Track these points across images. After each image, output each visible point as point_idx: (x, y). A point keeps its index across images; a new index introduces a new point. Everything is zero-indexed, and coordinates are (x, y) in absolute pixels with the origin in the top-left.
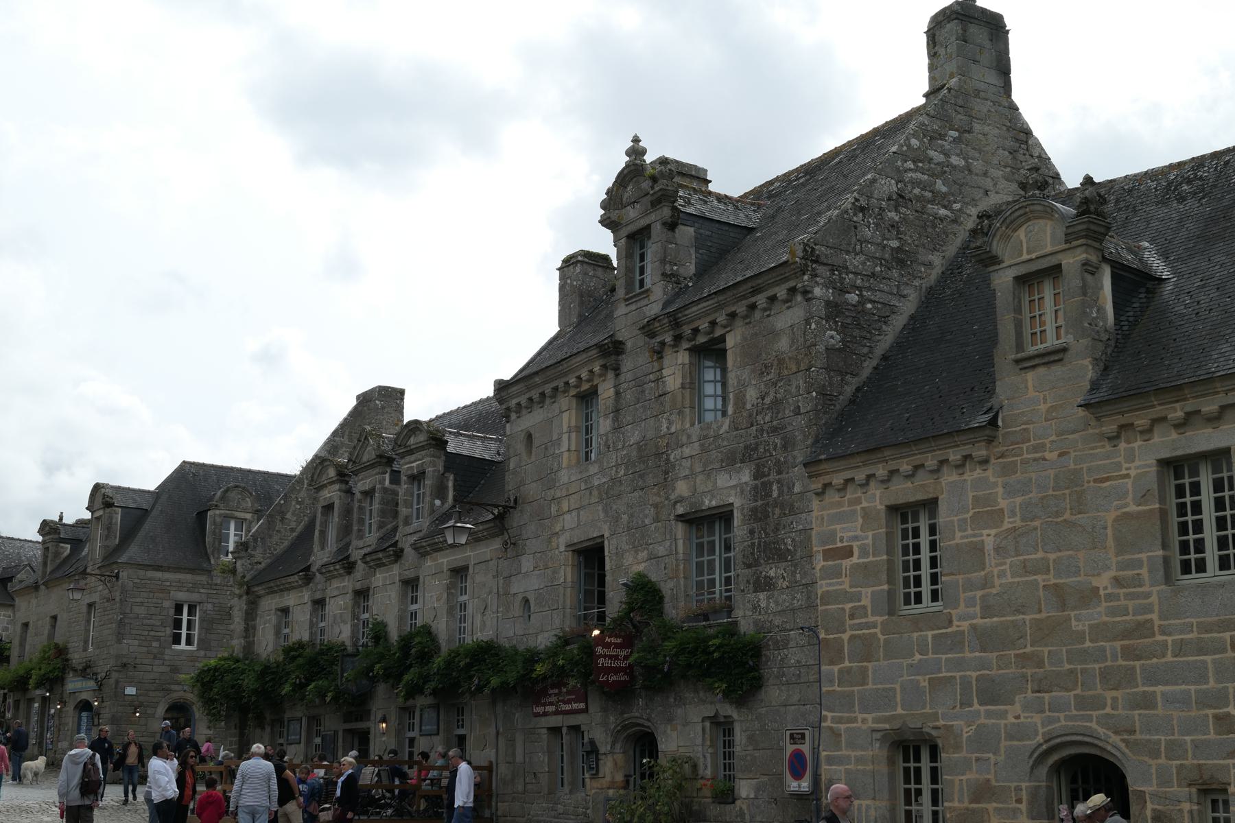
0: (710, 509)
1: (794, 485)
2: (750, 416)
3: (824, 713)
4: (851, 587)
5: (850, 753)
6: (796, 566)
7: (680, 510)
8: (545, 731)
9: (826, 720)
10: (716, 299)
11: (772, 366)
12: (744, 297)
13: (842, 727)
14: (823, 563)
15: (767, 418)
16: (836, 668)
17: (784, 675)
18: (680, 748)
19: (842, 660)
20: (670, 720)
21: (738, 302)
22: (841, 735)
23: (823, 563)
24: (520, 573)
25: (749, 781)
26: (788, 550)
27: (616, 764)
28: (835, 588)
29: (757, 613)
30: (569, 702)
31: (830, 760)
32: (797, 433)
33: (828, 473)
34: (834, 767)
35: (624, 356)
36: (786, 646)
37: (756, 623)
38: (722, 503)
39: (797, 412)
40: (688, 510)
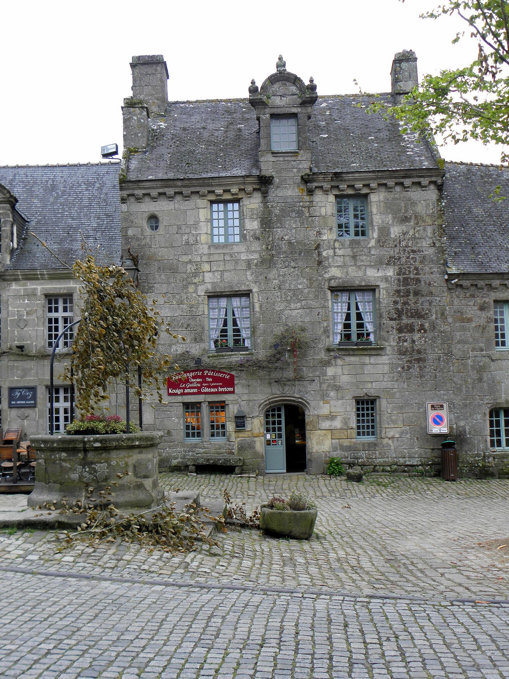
7: (333, 283)
11: (410, 218)
12: (396, 178)
30: (216, 387)
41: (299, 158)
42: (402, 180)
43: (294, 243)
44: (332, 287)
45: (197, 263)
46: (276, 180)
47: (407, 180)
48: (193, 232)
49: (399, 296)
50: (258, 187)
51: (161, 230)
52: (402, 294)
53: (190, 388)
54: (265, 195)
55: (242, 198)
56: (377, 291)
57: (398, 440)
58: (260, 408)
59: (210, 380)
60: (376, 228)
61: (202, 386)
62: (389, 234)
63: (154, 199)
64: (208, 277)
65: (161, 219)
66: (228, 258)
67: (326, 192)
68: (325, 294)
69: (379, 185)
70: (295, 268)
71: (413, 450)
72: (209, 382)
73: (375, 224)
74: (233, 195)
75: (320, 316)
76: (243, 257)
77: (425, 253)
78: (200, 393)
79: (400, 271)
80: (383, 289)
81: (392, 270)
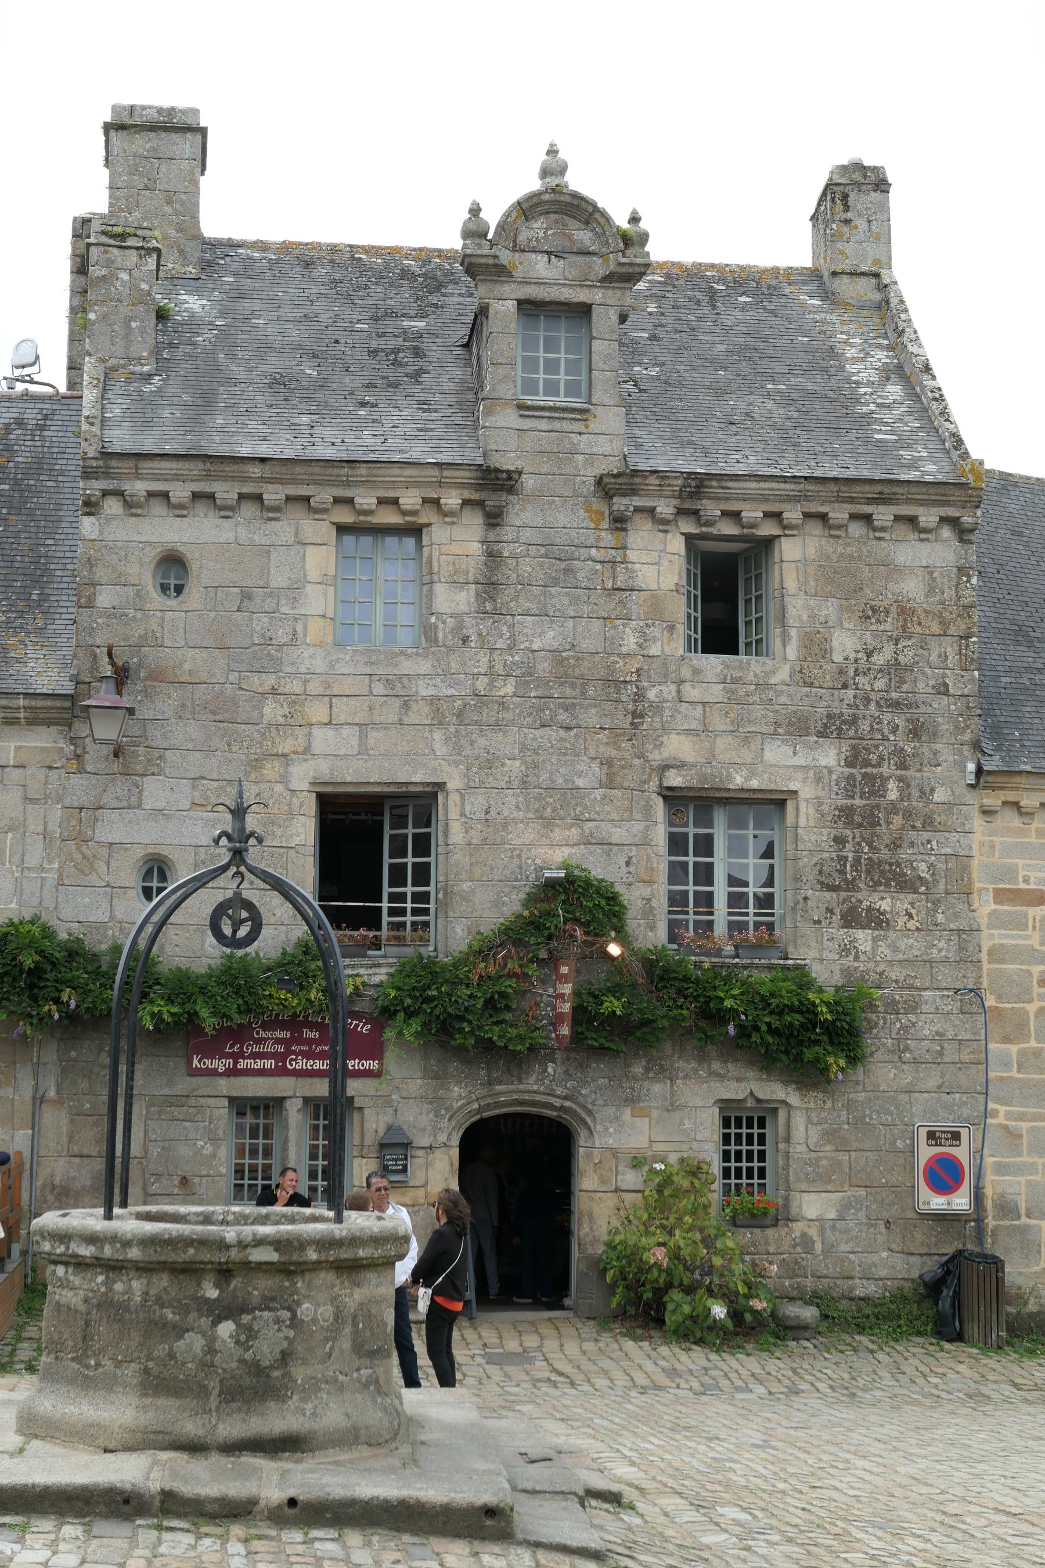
0: (742, 790)
1: (933, 790)
2: (841, 672)
3: (991, 1105)
4: (1041, 944)
5: (1036, 1159)
6: (936, 903)
7: (675, 779)
8: (225, 1102)
9: (995, 1114)
10: (802, 487)
11: (887, 613)
12: (852, 500)
13: (1024, 1125)
14: (993, 907)
15: (879, 685)
16: (1014, 1049)
17: (907, 1049)
18: (654, 1145)
19: (1026, 1038)
20: (631, 1101)
21: (837, 501)
22: (1021, 1136)
23: (993, 907)
24: (139, 806)
25: (823, 1195)
26: (920, 878)
27: (452, 1165)
28: (1014, 942)
29: (851, 958)
31: (1001, 1169)
32: (940, 720)
33: (1017, 789)
34: (1006, 1178)
35: (513, 498)
36: (913, 1008)
37: (846, 972)
38: (772, 787)
39: (943, 690)
40: (695, 783)
41: (593, 426)
42: (867, 509)
43: (568, 659)
44: (669, 789)
45: (295, 700)
46: (528, 482)
47: (881, 508)
48: (284, 609)
49: (850, 823)
50: (475, 496)
51: (194, 597)
52: (857, 819)
53: (255, 1056)
54: (494, 519)
55: (429, 525)
56: (790, 805)
57: (833, 1228)
58: (454, 1123)
59: (314, 1035)
60: (793, 632)
61: (288, 1052)
62: (826, 653)
63: (179, 509)
64: (323, 739)
65: (194, 567)
66: (379, 688)
67: (664, 524)
68: (648, 808)
69: (807, 515)
70: (569, 729)
71: (874, 1258)
72: (310, 1042)
73: (791, 622)
74: (404, 513)
75: (632, 869)
76: (425, 690)
77: (923, 709)
78: (282, 1071)
79: (855, 756)
80: (807, 800)
81: (832, 752)
